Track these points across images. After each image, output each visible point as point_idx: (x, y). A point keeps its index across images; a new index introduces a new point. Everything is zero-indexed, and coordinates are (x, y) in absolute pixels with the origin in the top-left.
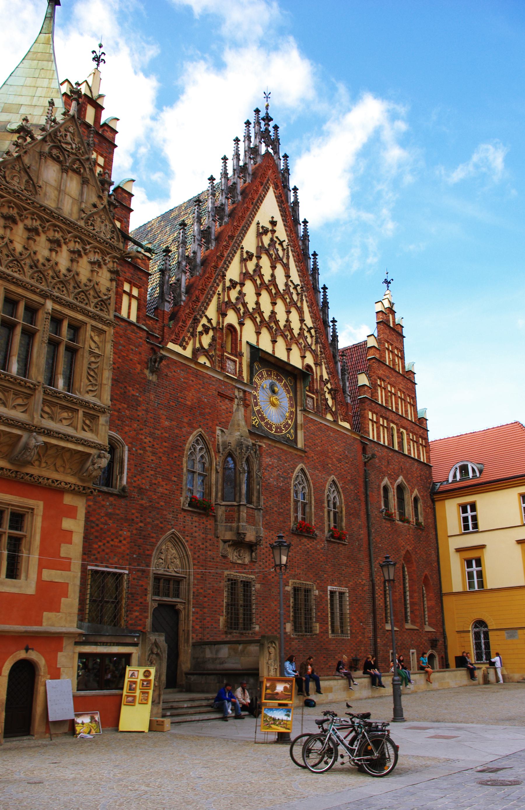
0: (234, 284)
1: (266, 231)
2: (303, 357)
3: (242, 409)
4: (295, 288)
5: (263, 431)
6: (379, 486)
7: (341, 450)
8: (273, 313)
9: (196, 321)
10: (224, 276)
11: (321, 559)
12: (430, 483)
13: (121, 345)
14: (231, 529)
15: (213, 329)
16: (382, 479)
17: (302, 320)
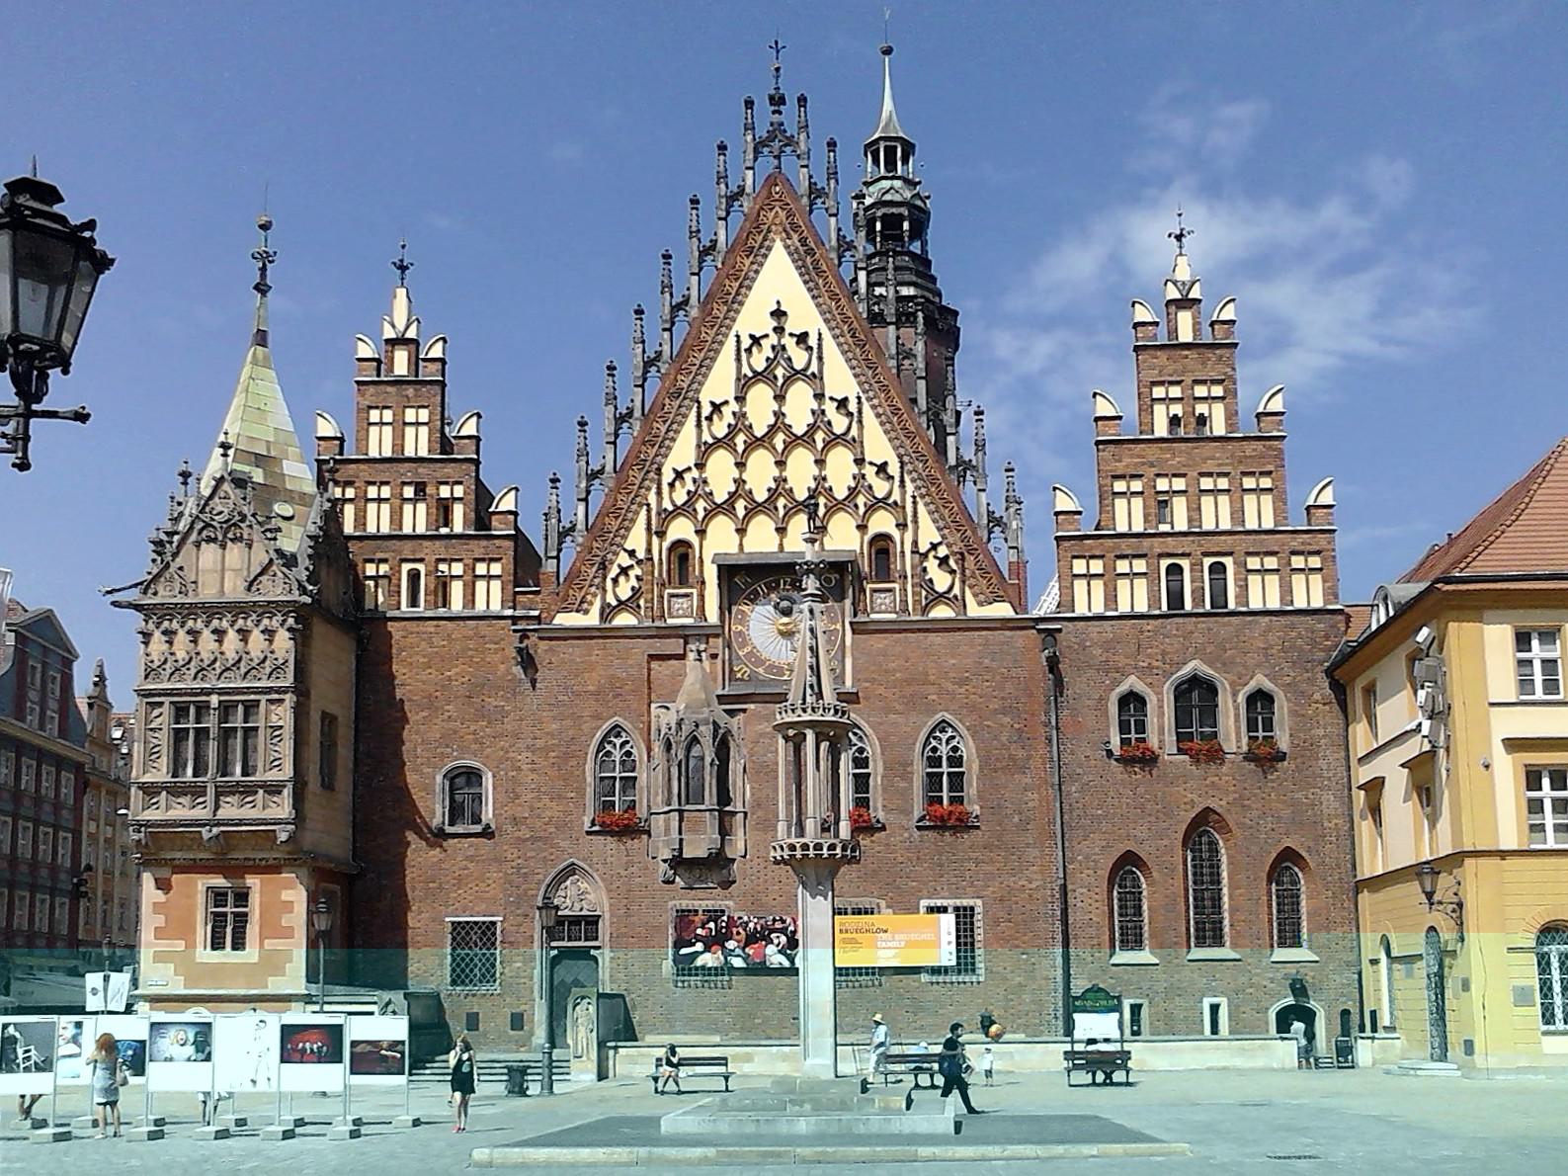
0: (679, 475)
1: (756, 340)
2: (862, 528)
3: (706, 664)
4: (842, 404)
5: (764, 682)
6: (1103, 700)
7: (964, 661)
8: (781, 480)
9: (604, 567)
10: (659, 471)
11: (900, 859)
12: (1329, 650)
13: (471, 649)
14: (667, 843)
15: (639, 562)
16: (1117, 683)
17: (860, 462)
